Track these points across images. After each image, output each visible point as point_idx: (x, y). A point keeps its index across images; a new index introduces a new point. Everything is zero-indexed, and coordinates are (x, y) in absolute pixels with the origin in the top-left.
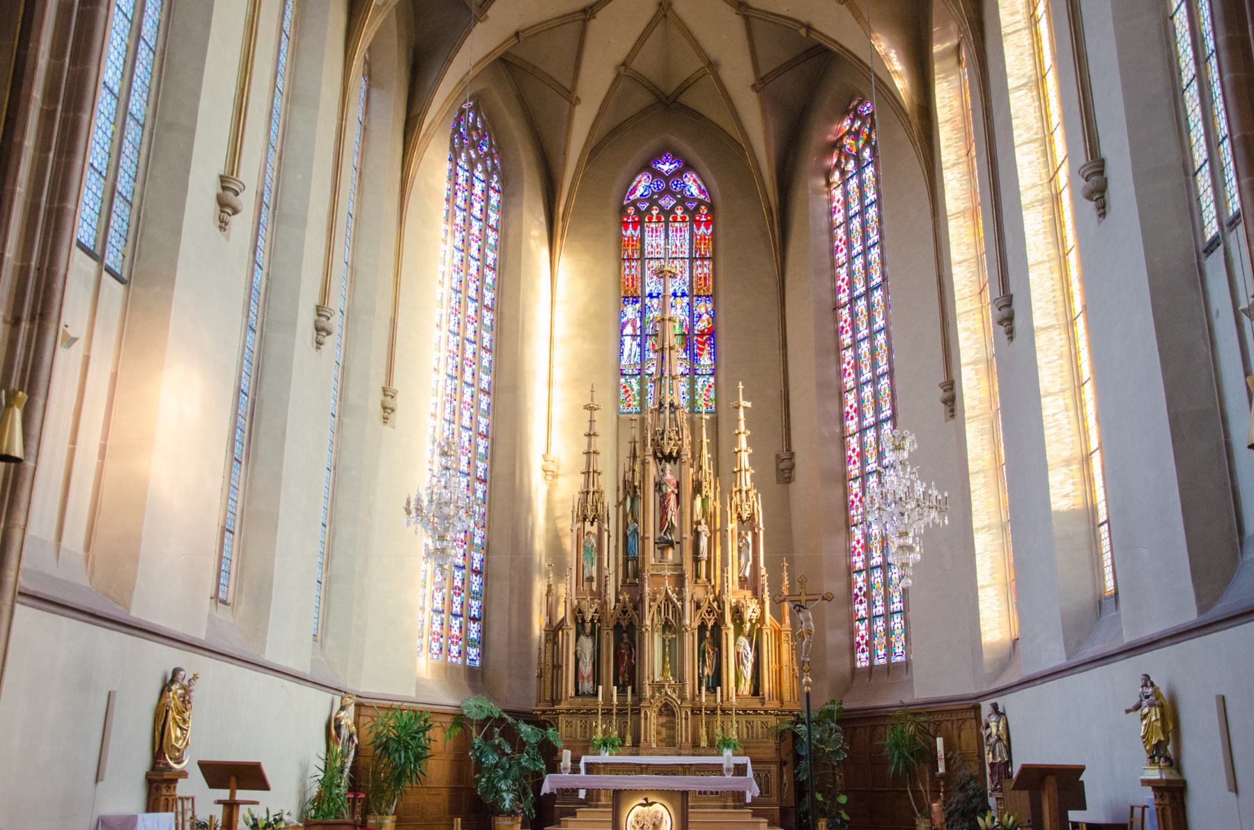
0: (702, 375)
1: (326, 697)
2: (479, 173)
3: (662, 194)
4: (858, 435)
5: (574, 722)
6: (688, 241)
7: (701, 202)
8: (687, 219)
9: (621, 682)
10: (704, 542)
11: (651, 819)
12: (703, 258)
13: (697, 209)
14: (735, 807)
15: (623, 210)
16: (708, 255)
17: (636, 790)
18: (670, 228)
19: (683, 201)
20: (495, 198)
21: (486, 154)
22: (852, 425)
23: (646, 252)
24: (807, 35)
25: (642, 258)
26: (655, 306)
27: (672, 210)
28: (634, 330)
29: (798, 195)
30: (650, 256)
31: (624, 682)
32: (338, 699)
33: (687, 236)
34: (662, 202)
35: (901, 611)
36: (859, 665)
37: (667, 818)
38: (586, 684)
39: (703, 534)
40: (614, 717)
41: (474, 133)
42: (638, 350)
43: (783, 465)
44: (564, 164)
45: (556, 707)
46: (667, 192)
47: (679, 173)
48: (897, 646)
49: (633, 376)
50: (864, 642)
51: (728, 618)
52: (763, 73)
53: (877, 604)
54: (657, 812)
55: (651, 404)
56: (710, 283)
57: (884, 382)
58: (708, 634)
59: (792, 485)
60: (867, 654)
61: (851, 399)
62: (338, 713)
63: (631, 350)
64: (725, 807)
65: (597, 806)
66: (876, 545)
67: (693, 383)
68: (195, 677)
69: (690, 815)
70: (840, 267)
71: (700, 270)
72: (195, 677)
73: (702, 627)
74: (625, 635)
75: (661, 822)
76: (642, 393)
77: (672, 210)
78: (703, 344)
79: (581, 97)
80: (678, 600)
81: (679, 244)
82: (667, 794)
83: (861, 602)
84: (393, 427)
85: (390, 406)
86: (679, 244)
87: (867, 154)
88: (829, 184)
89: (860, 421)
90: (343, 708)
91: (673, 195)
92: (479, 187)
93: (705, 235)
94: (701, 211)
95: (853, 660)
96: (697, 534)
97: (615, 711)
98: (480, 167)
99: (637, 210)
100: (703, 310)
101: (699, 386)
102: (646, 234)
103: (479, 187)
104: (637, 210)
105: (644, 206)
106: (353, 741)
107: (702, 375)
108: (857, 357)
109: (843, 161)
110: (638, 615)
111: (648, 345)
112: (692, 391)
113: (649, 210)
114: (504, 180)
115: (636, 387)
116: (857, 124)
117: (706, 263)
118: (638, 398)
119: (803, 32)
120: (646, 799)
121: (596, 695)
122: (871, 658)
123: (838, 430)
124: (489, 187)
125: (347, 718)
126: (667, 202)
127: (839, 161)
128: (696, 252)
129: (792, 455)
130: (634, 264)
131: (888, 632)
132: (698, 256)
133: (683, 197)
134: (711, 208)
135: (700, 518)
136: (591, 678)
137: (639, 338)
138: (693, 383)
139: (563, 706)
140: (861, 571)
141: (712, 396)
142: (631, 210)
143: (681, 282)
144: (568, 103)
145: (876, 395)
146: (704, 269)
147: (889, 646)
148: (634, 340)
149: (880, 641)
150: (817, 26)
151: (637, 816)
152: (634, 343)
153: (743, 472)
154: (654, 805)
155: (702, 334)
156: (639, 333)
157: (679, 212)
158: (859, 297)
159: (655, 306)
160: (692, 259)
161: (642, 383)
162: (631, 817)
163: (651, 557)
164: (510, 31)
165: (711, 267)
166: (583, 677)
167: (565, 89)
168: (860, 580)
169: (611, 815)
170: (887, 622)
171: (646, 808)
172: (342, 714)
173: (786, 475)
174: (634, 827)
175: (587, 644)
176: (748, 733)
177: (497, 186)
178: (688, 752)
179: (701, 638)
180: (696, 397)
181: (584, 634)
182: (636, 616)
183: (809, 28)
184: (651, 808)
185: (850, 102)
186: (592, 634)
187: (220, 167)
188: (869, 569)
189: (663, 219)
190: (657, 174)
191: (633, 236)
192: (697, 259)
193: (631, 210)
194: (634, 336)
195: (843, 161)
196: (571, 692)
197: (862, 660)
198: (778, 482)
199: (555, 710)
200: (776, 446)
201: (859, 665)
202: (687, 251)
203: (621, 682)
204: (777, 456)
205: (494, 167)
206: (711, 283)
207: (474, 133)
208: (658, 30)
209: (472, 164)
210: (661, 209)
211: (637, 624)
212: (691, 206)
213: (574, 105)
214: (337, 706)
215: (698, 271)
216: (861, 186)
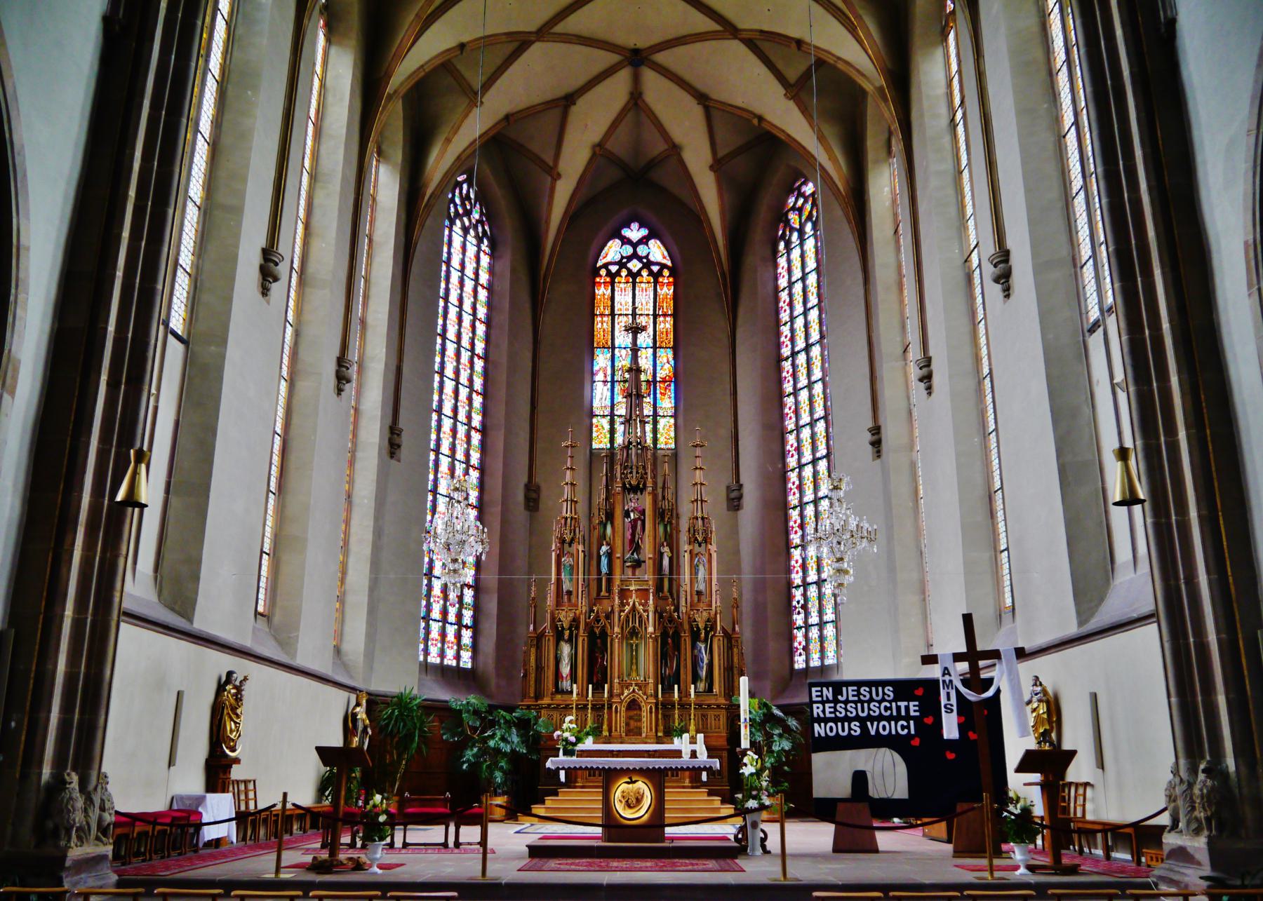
0: (664, 416)
1: (343, 695)
2: (471, 238)
3: (630, 258)
4: (797, 470)
5: (555, 716)
6: (652, 300)
7: (663, 266)
8: (652, 280)
9: (595, 681)
10: (666, 562)
11: (635, 794)
12: (665, 315)
13: (660, 273)
14: (692, 787)
15: (596, 272)
16: (670, 313)
17: (628, 769)
18: (637, 289)
19: (648, 264)
20: (485, 260)
21: (478, 221)
22: (792, 462)
23: (616, 309)
24: (759, 124)
25: (613, 314)
26: (624, 356)
27: (639, 273)
28: (606, 377)
30: (619, 313)
31: (597, 681)
32: (353, 697)
33: (652, 296)
34: (630, 265)
35: (832, 621)
36: (797, 666)
37: (647, 793)
38: (565, 682)
39: (665, 554)
40: (589, 711)
41: (467, 203)
42: (609, 394)
43: (734, 495)
44: (547, 231)
45: (539, 702)
46: (635, 256)
47: (644, 241)
48: (829, 650)
49: (604, 416)
50: (801, 647)
51: (686, 626)
52: (721, 154)
53: (812, 614)
54: (639, 789)
55: (619, 440)
56: (671, 336)
57: (821, 426)
58: (670, 640)
59: (740, 512)
60: (804, 657)
61: (791, 439)
62: (354, 709)
63: (602, 394)
64: (684, 787)
65: (575, 787)
66: (812, 565)
68: (246, 679)
69: (666, 795)
70: (784, 325)
71: (662, 325)
72: (246, 679)
73: (664, 635)
74: (599, 641)
75: (642, 796)
76: (612, 431)
77: (639, 273)
78: (666, 389)
79: (562, 173)
80: (645, 611)
81: (644, 303)
82: (647, 773)
83: (799, 613)
84: (399, 461)
85: (397, 442)
86: (644, 303)
87: (808, 227)
88: (775, 252)
89: (799, 460)
90: (358, 704)
91: (640, 259)
92: (471, 250)
93: (667, 294)
94: (664, 274)
95: (792, 662)
97: (590, 706)
98: (472, 232)
99: (609, 273)
100: (665, 360)
101: (660, 426)
102: (616, 293)
103: (471, 250)
104: (609, 273)
105: (614, 269)
106: (367, 733)
107: (664, 416)
108: (797, 403)
109: (788, 233)
110: (610, 624)
111: (617, 388)
112: (655, 431)
113: (618, 273)
114: (492, 246)
115: (607, 427)
116: (801, 201)
117: (668, 319)
118: (608, 436)
119: (755, 121)
120: (630, 778)
121: (571, 692)
122: (807, 661)
123: (780, 466)
124: (479, 249)
125: (361, 713)
126: (635, 265)
127: (784, 233)
128: (659, 309)
129: (741, 486)
130: (605, 319)
131: (822, 638)
132: (660, 313)
133: (648, 260)
135: (663, 540)
136: (569, 678)
137: (609, 384)
138: (655, 423)
139: (546, 701)
140: (799, 586)
141: (672, 434)
142: (603, 272)
143: (646, 335)
144: (549, 179)
145: (813, 436)
146: (666, 324)
147: (822, 650)
148: (605, 385)
149: (815, 647)
150: (769, 117)
151: (623, 792)
152: (606, 388)
153: (699, 502)
154: (637, 783)
155: (664, 381)
156: (609, 379)
157: (645, 273)
158: (799, 352)
159: (624, 356)
160: (655, 316)
161: (612, 423)
162: (618, 794)
164: (501, 115)
165: (672, 322)
166: (562, 677)
167: (548, 165)
168: (798, 594)
169: (601, 794)
170: (821, 630)
171: (631, 786)
172: (358, 709)
173: (735, 504)
174: (620, 801)
175: (566, 649)
176: (703, 725)
177: (487, 250)
178: (652, 741)
179: (664, 644)
180: (658, 436)
181: (564, 640)
182: (608, 625)
183: (761, 118)
184: (634, 785)
185: (794, 183)
186: (570, 641)
187: (262, 241)
188: (805, 585)
189: (631, 280)
190: (626, 241)
191: (604, 294)
192: (660, 316)
193: (603, 272)
194: (605, 382)
195: (788, 233)
196: (551, 688)
197: (800, 663)
198: (728, 510)
199: (538, 705)
200: (727, 479)
201: (797, 666)
202: (652, 309)
203: (595, 681)
204: (728, 488)
205: (484, 231)
206: (672, 337)
207: (467, 203)
208: (630, 117)
209: (465, 230)
210: (629, 271)
211: (609, 632)
212: (655, 268)
213: (556, 180)
214: (353, 703)
215: (660, 327)
216: (803, 256)
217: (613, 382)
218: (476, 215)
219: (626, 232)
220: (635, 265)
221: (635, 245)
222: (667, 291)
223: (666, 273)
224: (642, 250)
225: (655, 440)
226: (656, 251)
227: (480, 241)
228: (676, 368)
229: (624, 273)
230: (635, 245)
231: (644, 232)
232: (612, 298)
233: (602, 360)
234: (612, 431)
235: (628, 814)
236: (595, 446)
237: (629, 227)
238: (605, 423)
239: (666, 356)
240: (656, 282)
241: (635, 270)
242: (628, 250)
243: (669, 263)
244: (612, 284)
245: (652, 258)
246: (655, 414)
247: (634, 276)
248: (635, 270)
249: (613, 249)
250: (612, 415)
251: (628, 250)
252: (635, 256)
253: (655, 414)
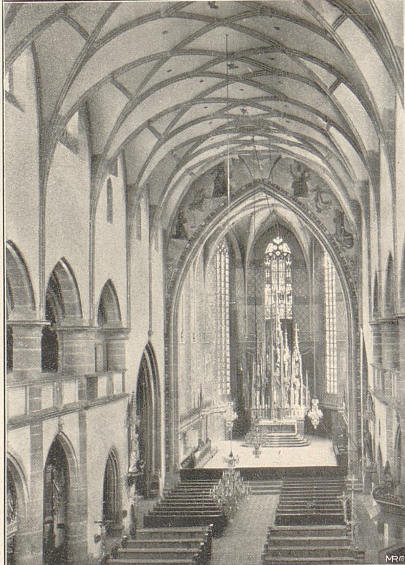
2: (222, 255)
3: (276, 251)
7: (288, 253)
19: (282, 253)
46: (278, 250)
47: (281, 244)
91: (280, 251)
103: (223, 260)
105: (271, 254)
142: (267, 256)
146: (289, 275)
161: (271, 310)
190: (275, 244)
218: (223, 246)
219: (275, 240)
221: (278, 245)
224: (281, 248)
226: (285, 248)
227: (224, 254)
230: (278, 245)
231: (281, 240)
236: (266, 318)
237: (276, 238)
241: (278, 255)
242: (275, 248)
243: (290, 252)
245: (284, 251)
248: (278, 255)
249: (271, 247)
251: (275, 248)
252: (278, 250)
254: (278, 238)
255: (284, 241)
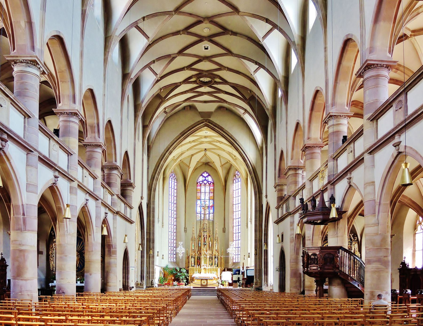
3: (204, 180)
7: (211, 182)
13: (210, 184)
15: (197, 183)
19: (208, 182)
25: (201, 192)
27: (206, 184)
29: (228, 183)
46: (205, 180)
47: (207, 176)
55: (202, 218)
56: (213, 197)
67: (209, 215)
76: (201, 217)
77: (206, 184)
91: (206, 180)
96: (209, 243)
99: (200, 184)
101: (210, 216)
105: (201, 183)
112: (209, 216)
113: (202, 184)
115: (200, 216)
126: (205, 182)
134: (213, 183)
138: (209, 215)
142: (199, 183)
155: (211, 206)
157: (207, 183)
160: (209, 193)
161: (201, 215)
163: (202, 247)
190: (203, 176)
212: (210, 183)
215: (211, 195)
217: (201, 207)
219: (203, 175)
220: (205, 182)
222: (212, 188)
223: (212, 184)
224: (207, 179)
225: (209, 218)
228: (213, 204)
229: (203, 183)
231: (207, 175)
232: (201, 189)
233: (199, 202)
234: (201, 217)
235: (204, 284)
238: (199, 215)
239: (211, 201)
240: (210, 186)
242: (204, 179)
244: (201, 186)
245: (209, 180)
246: (209, 213)
247: (205, 184)
250: (201, 213)
251: (204, 179)
252: (205, 180)
253: (209, 213)
254: (205, 173)
255: (209, 175)
